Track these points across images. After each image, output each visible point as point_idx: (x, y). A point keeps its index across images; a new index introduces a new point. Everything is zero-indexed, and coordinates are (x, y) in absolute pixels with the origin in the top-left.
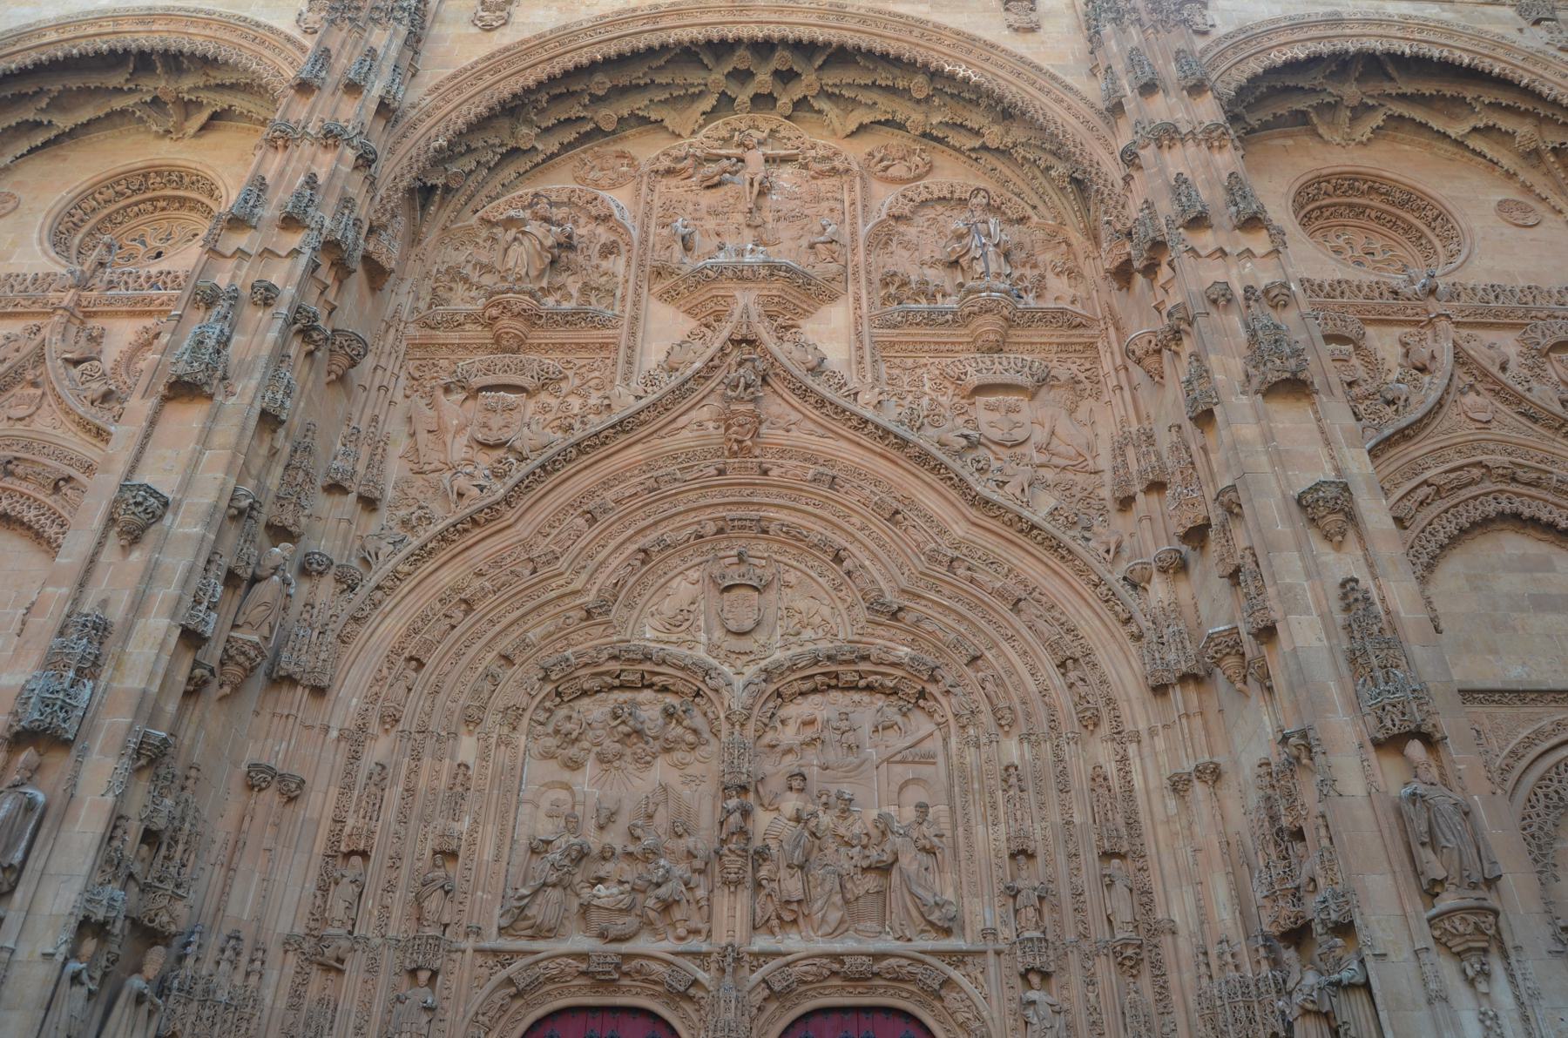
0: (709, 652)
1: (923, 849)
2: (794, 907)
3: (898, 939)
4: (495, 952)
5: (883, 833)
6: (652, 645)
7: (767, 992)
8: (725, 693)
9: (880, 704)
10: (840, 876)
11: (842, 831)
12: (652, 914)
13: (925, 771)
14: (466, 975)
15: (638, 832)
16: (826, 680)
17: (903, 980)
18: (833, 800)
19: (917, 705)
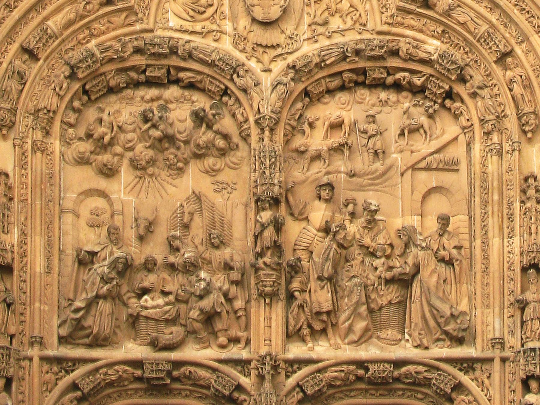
0: (236, 45)
1: (442, 260)
2: (324, 317)
3: (416, 347)
4: (59, 360)
5: (407, 246)
6: (177, 35)
7: (301, 394)
8: (255, 95)
9: (407, 105)
10: (366, 286)
11: (367, 241)
12: (197, 325)
13: (446, 178)
14: (36, 380)
15: (177, 243)
16: (354, 77)
17: (419, 385)
18: (360, 209)
19: (443, 106)
